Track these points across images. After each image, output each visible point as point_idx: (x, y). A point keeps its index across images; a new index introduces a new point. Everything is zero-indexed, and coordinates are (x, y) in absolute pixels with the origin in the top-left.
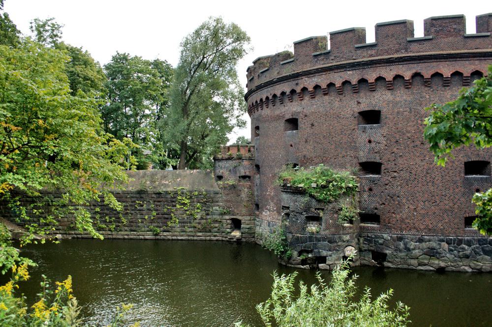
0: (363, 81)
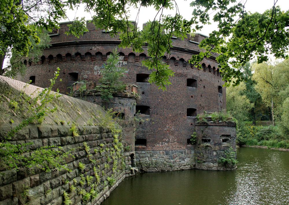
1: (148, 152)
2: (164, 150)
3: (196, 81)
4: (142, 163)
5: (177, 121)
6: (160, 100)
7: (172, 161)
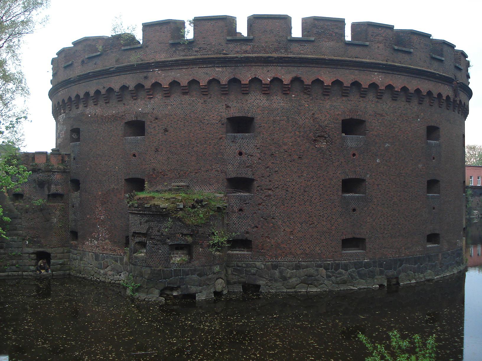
0: (235, 81)
5: (109, 203)
6: (88, 169)
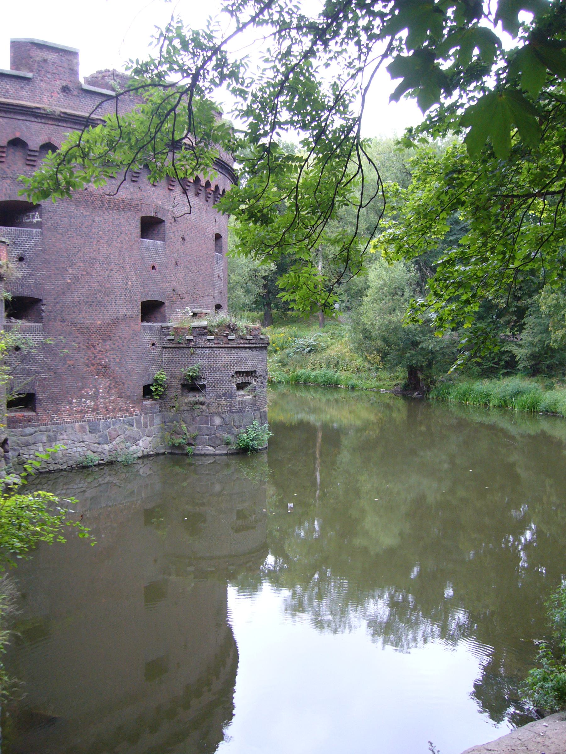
1: (43, 428)
2: (84, 421)
3: (163, 221)
4: (25, 460)
6: (69, 281)
7: (107, 447)
